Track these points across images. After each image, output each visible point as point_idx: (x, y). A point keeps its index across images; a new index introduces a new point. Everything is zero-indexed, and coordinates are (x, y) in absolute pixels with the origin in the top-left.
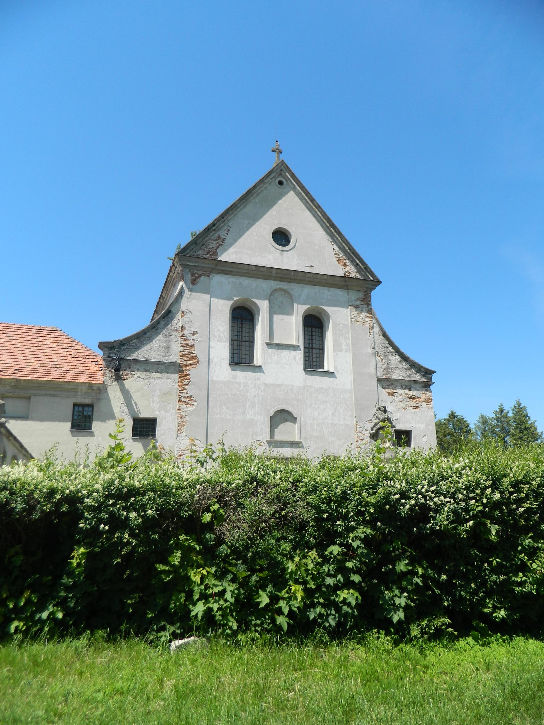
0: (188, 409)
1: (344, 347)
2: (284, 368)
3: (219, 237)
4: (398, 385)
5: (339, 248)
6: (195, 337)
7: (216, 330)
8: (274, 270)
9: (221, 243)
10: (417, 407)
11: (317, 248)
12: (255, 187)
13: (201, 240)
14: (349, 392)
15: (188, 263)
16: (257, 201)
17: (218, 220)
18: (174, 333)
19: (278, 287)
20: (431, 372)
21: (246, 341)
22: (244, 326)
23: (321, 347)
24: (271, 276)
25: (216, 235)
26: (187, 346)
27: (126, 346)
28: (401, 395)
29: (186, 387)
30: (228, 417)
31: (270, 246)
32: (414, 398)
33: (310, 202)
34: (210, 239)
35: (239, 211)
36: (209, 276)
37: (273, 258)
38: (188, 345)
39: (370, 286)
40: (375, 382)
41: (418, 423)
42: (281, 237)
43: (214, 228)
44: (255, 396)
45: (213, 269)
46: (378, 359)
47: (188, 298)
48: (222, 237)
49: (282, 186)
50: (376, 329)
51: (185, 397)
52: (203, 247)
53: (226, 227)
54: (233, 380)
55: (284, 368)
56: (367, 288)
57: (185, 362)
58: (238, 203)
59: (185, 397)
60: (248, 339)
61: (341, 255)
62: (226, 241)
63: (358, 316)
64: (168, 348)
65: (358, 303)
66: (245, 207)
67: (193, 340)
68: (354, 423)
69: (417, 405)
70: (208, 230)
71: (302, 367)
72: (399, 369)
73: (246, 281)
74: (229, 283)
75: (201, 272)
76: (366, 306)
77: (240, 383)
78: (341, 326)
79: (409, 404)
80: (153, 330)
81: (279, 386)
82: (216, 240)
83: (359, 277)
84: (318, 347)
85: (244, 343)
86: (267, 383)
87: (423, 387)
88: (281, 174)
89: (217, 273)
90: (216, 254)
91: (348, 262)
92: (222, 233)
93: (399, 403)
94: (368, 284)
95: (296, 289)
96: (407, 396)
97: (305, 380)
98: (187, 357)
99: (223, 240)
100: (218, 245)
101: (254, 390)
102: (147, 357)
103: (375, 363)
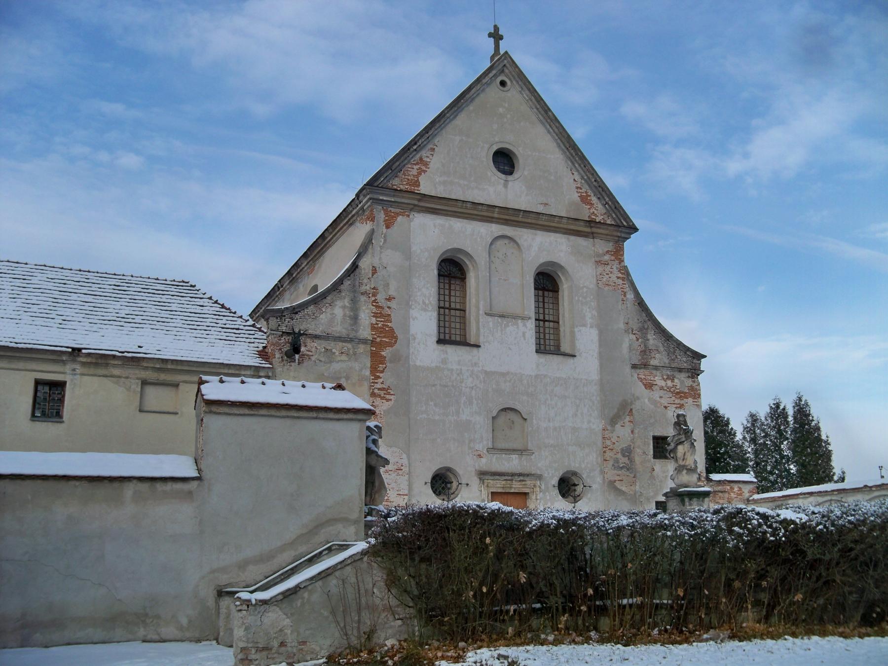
3: (421, 159)
5: (582, 178)
7: (419, 294)
8: (497, 210)
9: (424, 168)
11: (552, 178)
13: (398, 163)
15: (381, 198)
16: (471, 108)
17: (420, 135)
18: (363, 298)
19: (500, 233)
20: (699, 356)
21: (456, 309)
22: (453, 287)
23: (556, 319)
24: (493, 218)
25: (418, 156)
27: (300, 314)
28: (662, 388)
29: (381, 375)
30: (437, 418)
31: (489, 174)
32: (678, 393)
33: (543, 112)
36: (408, 216)
37: (495, 190)
38: (382, 315)
39: (623, 235)
40: (628, 369)
42: (504, 160)
43: (415, 147)
44: (472, 388)
45: (415, 205)
48: (425, 159)
49: (505, 89)
50: (630, 296)
51: (379, 389)
52: (400, 174)
53: (430, 146)
57: (378, 340)
59: (379, 389)
60: (458, 307)
61: (586, 188)
62: (431, 165)
64: (355, 318)
65: (607, 257)
67: (389, 308)
68: (601, 427)
69: (682, 402)
70: (406, 149)
71: (533, 348)
72: (659, 352)
73: (457, 224)
74: (435, 226)
75: (398, 210)
76: (617, 261)
77: (452, 370)
78: (585, 290)
80: (335, 293)
81: (504, 375)
83: (609, 222)
84: (551, 319)
85: (453, 312)
89: (419, 212)
90: (417, 184)
91: (594, 200)
92: (424, 153)
93: (658, 399)
94: (621, 232)
95: (525, 236)
97: (538, 366)
99: (426, 164)
100: (421, 172)
101: (470, 379)
102: (330, 331)
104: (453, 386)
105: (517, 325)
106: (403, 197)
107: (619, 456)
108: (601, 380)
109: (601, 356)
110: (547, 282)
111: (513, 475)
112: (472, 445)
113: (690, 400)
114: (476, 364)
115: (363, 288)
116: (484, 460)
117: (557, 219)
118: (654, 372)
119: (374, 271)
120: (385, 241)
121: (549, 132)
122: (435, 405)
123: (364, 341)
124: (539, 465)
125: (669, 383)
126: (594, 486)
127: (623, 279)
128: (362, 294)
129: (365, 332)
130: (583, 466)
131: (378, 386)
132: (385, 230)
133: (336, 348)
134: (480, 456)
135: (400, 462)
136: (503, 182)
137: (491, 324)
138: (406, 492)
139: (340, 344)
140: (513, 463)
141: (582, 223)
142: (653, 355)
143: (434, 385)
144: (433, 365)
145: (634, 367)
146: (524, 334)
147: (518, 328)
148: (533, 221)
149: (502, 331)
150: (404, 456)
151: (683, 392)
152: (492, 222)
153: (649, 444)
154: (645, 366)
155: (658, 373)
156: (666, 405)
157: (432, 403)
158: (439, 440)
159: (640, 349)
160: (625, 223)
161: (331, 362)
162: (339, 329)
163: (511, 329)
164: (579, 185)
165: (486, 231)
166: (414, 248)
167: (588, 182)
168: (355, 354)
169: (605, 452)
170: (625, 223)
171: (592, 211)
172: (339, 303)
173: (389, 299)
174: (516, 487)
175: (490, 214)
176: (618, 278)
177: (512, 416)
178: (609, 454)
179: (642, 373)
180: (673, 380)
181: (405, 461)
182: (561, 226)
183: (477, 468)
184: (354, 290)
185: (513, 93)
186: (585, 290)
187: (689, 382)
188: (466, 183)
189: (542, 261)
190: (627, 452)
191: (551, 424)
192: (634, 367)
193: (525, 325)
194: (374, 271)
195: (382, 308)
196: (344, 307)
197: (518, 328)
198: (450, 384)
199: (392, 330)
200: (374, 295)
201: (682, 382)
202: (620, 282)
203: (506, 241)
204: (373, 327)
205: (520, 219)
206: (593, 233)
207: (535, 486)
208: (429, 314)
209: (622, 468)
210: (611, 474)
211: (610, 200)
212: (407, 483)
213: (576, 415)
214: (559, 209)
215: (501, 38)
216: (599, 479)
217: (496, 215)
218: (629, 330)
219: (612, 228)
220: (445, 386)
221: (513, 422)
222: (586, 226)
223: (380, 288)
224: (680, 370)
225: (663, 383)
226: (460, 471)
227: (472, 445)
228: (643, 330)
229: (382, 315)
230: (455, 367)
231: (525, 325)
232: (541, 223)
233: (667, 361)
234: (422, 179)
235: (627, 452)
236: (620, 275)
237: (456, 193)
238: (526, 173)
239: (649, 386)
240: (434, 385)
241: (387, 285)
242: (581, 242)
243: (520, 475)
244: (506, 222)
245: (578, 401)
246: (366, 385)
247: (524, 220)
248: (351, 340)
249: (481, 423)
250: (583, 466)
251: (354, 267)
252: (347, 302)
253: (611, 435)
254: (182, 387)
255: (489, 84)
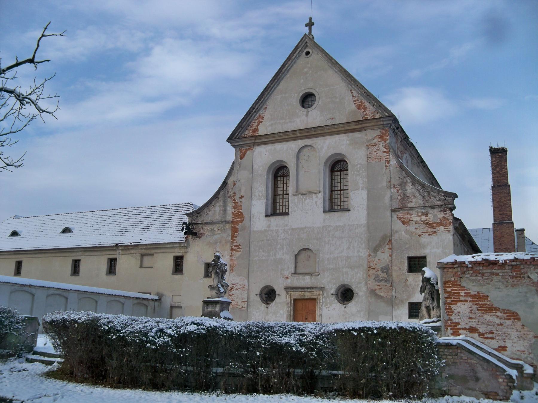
0: (236, 255)
1: (361, 185)
2: (307, 213)
3: (260, 116)
4: (414, 213)
6: (243, 200)
8: (298, 132)
9: (261, 120)
10: (434, 233)
11: (338, 100)
12: (283, 66)
13: (245, 123)
14: (364, 226)
16: (288, 76)
17: (256, 103)
18: (229, 199)
19: (303, 145)
25: (258, 115)
26: (238, 207)
27: (201, 213)
28: (417, 222)
29: (236, 238)
34: (253, 119)
35: (275, 89)
38: (237, 207)
40: (388, 213)
41: (434, 248)
44: (284, 239)
45: (254, 143)
46: (393, 190)
47: (238, 170)
54: (268, 229)
55: (307, 213)
56: (383, 125)
57: (235, 220)
58: (272, 84)
59: (235, 246)
63: (375, 153)
64: (225, 211)
65: (375, 141)
66: (278, 84)
67: (241, 202)
68: (367, 254)
69: (434, 230)
73: (279, 146)
74: (266, 151)
77: (273, 230)
78: (359, 166)
79: (425, 230)
81: (302, 229)
82: (258, 119)
83: (378, 116)
86: (294, 227)
87: (441, 211)
88: (307, 46)
90: (257, 130)
91: (367, 105)
92: (261, 112)
93: (414, 230)
94: (383, 121)
96: (423, 222)
98: (237, 216)
99: (262, 118)
101: (283, 234)
103: (389, 196)
104: (273, 239)
105: (312, 197)
106: (247, 141)
107: (380, 272)
108: (368, 223)
109: (368, 208)
110: (337, 166)
111: (303, 288)
112: (283, 272)
113: (442, 228)
114: (287, 225)
115: (230, 194)
116: (289, 281)
117: (336, 126)
118: (411, 212)
119: (235, 184)
120: (240, 166)
121: (336, 72)
122: (263, 251)
123: (228, 222)
124: (323, 282)
125: (424, 218)
126: (360, 294)
127: (388, 152)
128: (229, 197)
129: (229, 217)
130: (353, 281)
131: (234, 244)
132: (240, 161)
133: (216, 227)
134: (287, 278)
135: (244, 284)
136: (305, 113)
137: (296, 200)
138: (246, 300)
139: (218, 225)
140: (307, 281)
141: (354, 124)
142: (410, 200)
143: (263, 240)
144: (263, 229)
145: (393, 210)
146: (316, 202)
147: (312, 200)
148: (322, 132)
149: (302, 203)
150: (246, 281)
151: (435, 223)
152: (298, 139)
153: (404, 263)
154: (402, 209)
155: (414, 212)
156: (420, 234)
157: (261, 251)
158: (264, 271)
159: (399, 197)
160: (387, 114)
161: (213, 235)
162: (218, 217)
163: (308, 201)
164: (356, 99)
165: (294, 146)
166: (255, 166)
167: (362, 95)
168: (224, 229)
169: (369, 270)
170: (387, 114)
171: (365, 113)
172: (218, 204)
173: (241, 197)
174: (308, 295)
175: (295, 136)
176: (383, 152)
177: (308, 253)
178: (372, 272)
179: (401, 214)
180: (426, 216)
181: (246, 283)
182: (340, 129)
183: (285, 285)
184: (225, 196)
185: (315, 56)
186: (359, 166)
187: (442, 215)
188: (284, 121)
189: (329, 154)
190: (387, 270)
191: (332, 256)
192: (393, 210)
193: (317, 197)
194: (235, 184)
195: (237, 203)
196: (220, 206)
197: (312, 200)
198: (271, 239)
199: (242, 214)
200: (234, 197)
201: (435, 216)
202: (385, 154)
203: (309, 148)
204: (234, 214)
205: (313, 133)
206: (363, 127)
207: (319, 295)
208: (261, 201)
209: (381, 281)
210: (373, 285)
211: (375, 102)
212: (246, 295)
213: (349, 248)
214: (341, 118)
215: (313, 24)
216: (364, 289)
217: (298, 135)
218: (391, 185)
219: (375, 121)
220: (268, 240)
221: (310, 257)
222: (357, 125)
223: (237, 193)
224: (433, 207)
225: (418, 219)
226: (275, 288)
227: (283, 272)
228: (403, 185)
229: (237, 207)
230: (275, 228)
231: (317, 197)
232: (327, 131)
233: (421, 202)
234: (260, 127)
235: (387, 270)
236: (385, 150)
237: (279, 129)
238: (320, 103)
239: (406, 222)
240: (263, 240)
241: (240, 190)
242: (357, 135)
243: (310, 288)
244: (307, 137)
245: (351, 240)
246: (229, 244)
247: (316, 133)
248: (221, 222)
249: (289, 260)
250: (353, 281)
251: (225, 183)
252: (221, 203)
253: (374, 259)
254: (155, 255)
255: (299, 57)
